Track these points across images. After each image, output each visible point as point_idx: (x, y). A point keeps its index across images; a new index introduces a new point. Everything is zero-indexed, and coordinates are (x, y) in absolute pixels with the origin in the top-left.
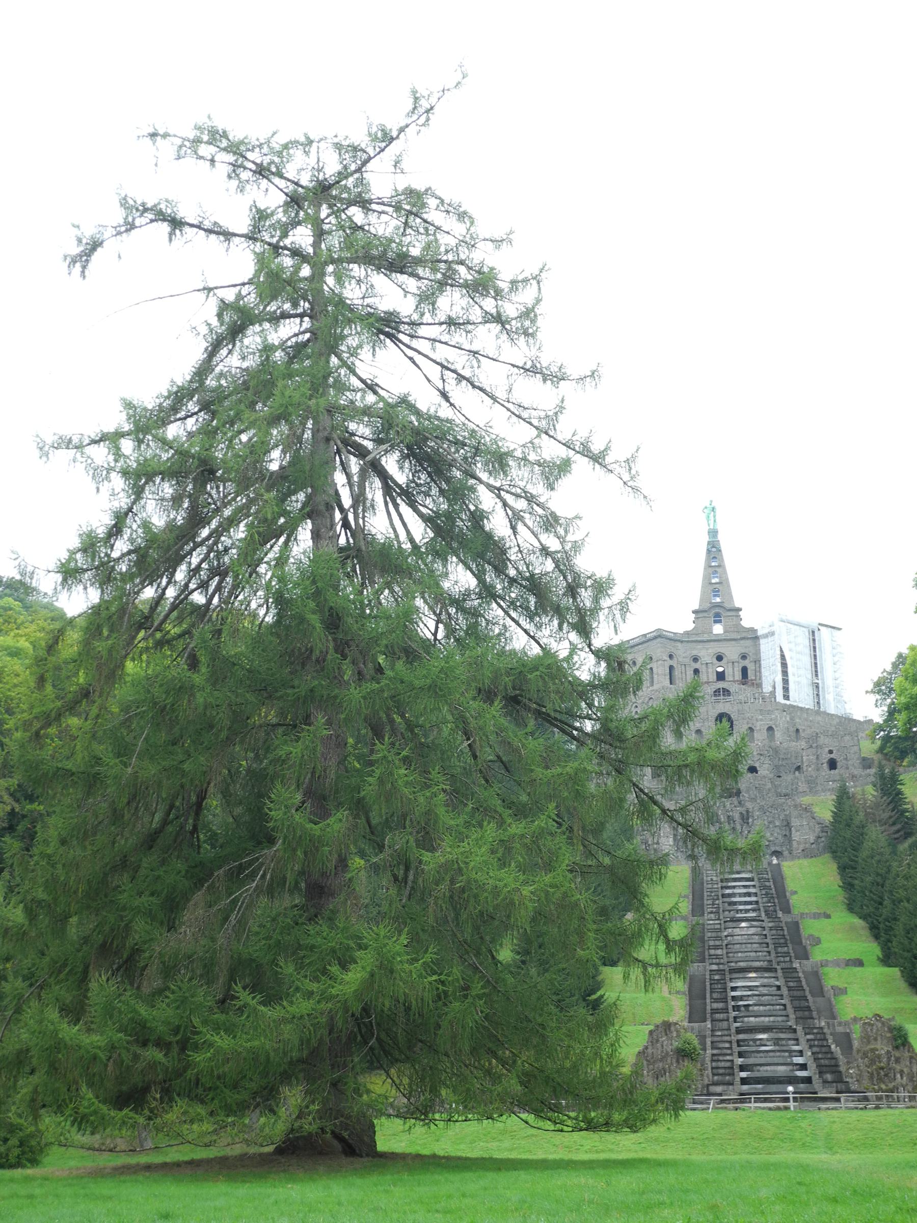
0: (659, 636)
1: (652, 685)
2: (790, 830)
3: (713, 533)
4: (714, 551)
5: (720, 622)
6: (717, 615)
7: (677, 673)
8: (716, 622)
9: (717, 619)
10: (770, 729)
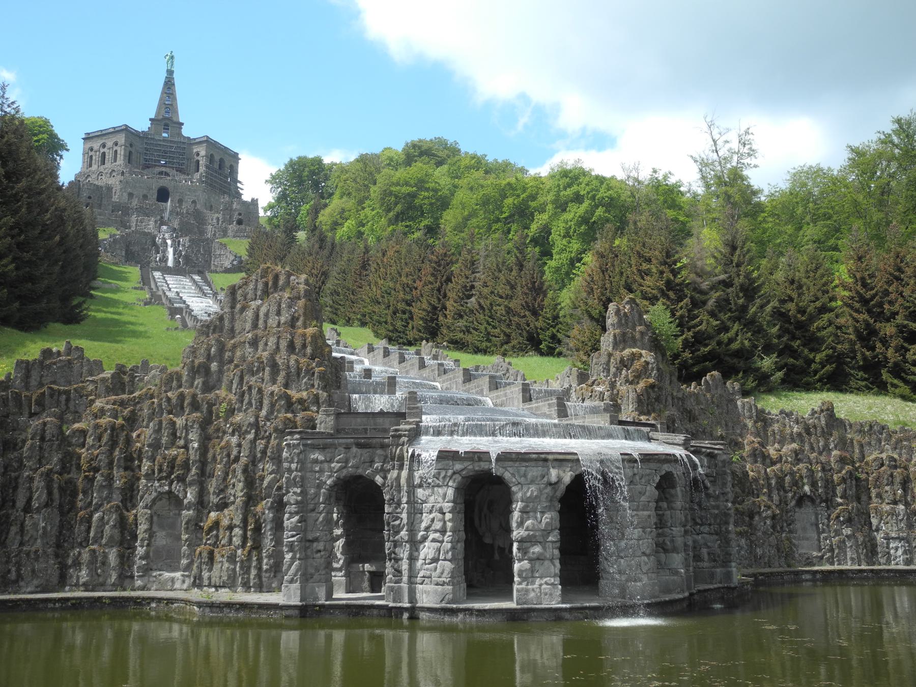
0: (126, 130)
1: (115, 160)
2: (211, 257)
3: (170, 73)
4: (169, 84)
5: (168, 129)
6: (167, 125)
7: (133, 157)
8: (164, 129)
9: (166, 128)
10: (194, 202)
